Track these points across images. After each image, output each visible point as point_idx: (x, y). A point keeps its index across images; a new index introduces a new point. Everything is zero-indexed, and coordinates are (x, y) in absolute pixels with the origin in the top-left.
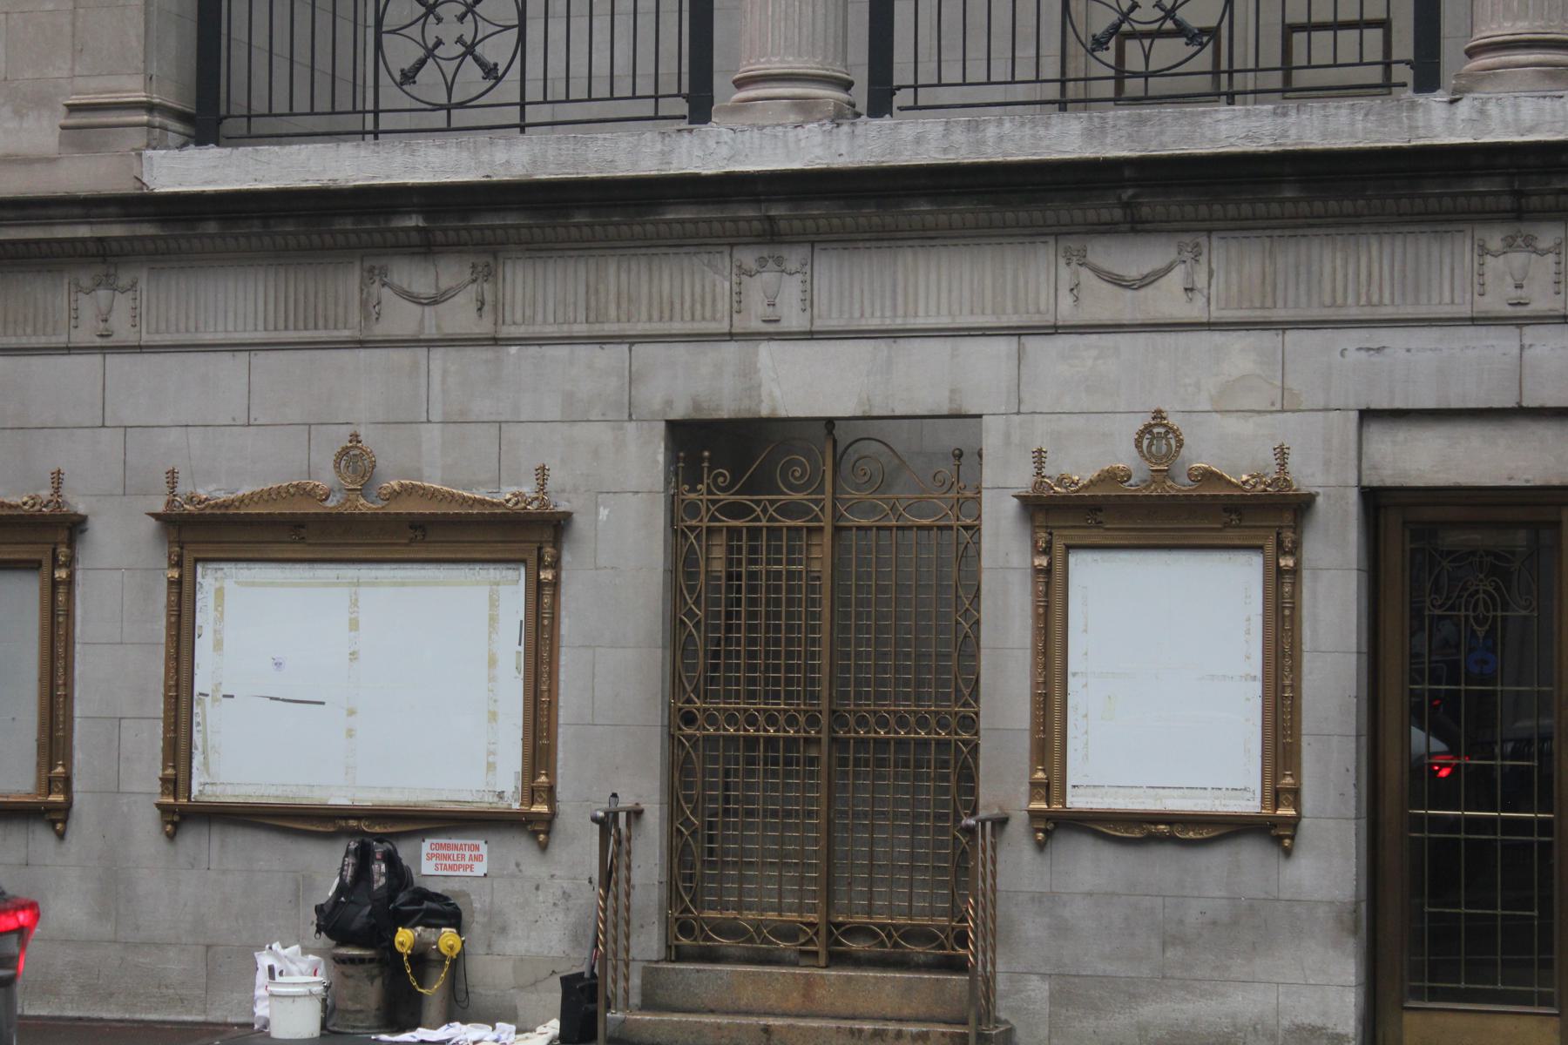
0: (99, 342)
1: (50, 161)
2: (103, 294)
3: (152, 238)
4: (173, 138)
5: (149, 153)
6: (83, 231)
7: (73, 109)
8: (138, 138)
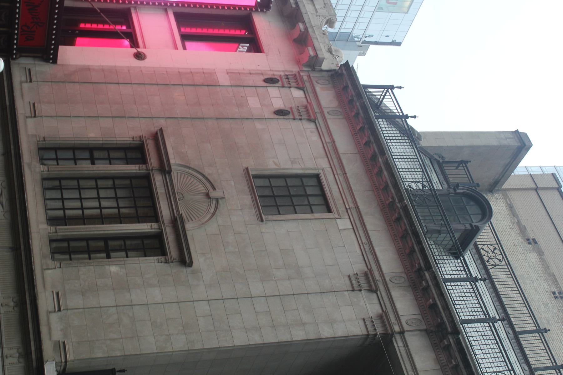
0: (4, 355)
1: (50, 339)
2: (17, 355)
3: (33, 366)
4: (59, 368)
5: (54, 363)
6: (33, 348)
7: (64, 343)
8: (58, 360)
